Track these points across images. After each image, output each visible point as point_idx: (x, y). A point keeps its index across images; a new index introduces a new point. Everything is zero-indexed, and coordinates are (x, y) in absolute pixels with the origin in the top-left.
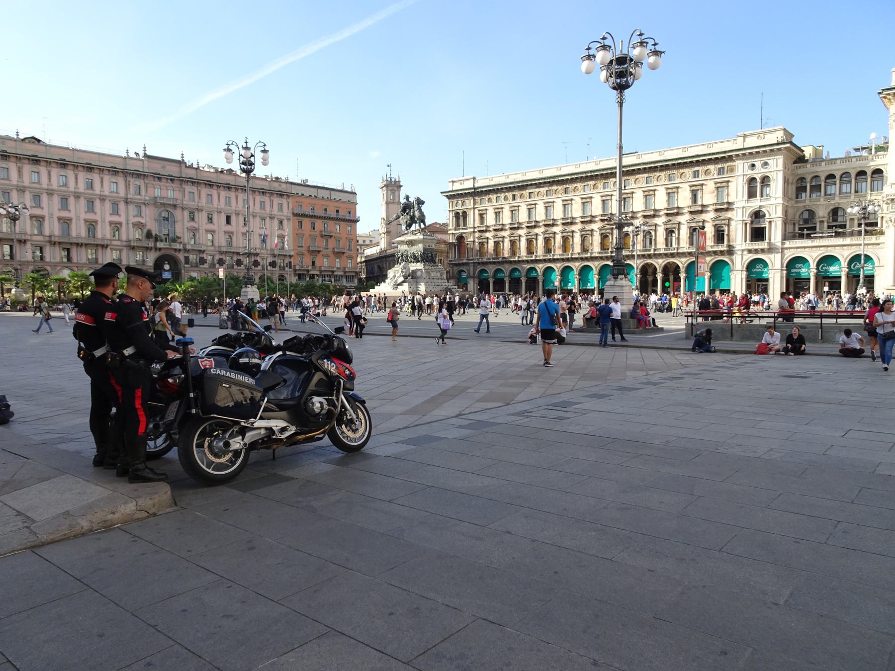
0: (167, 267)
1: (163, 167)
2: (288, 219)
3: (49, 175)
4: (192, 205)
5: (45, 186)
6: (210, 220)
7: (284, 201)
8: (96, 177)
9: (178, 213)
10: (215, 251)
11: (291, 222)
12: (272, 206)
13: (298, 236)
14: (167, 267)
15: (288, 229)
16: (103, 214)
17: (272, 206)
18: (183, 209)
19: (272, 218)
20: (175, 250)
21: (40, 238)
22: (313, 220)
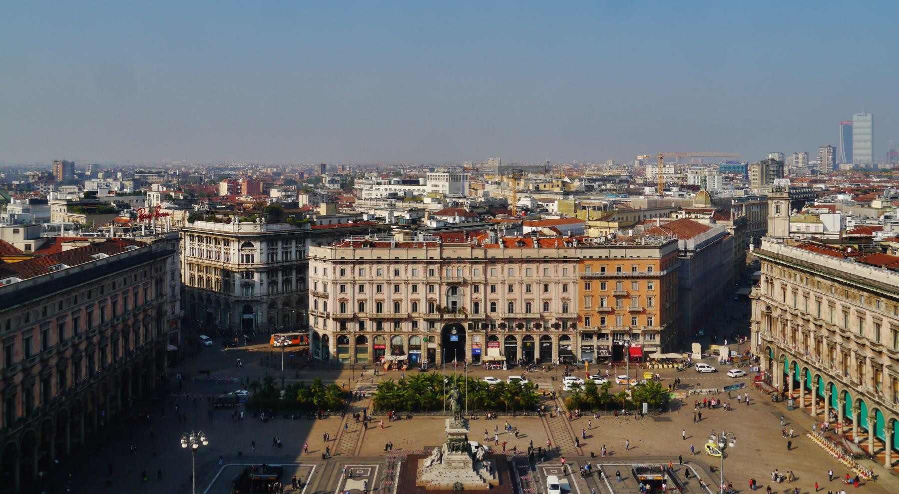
0: (454, 332)
2: (575, 283)
4: (475, 280)
5: (368, 278)
7: (570, 266)
8: (401, 267)
14: (454, 332)
15: (573, 292)
22: (604, 281)
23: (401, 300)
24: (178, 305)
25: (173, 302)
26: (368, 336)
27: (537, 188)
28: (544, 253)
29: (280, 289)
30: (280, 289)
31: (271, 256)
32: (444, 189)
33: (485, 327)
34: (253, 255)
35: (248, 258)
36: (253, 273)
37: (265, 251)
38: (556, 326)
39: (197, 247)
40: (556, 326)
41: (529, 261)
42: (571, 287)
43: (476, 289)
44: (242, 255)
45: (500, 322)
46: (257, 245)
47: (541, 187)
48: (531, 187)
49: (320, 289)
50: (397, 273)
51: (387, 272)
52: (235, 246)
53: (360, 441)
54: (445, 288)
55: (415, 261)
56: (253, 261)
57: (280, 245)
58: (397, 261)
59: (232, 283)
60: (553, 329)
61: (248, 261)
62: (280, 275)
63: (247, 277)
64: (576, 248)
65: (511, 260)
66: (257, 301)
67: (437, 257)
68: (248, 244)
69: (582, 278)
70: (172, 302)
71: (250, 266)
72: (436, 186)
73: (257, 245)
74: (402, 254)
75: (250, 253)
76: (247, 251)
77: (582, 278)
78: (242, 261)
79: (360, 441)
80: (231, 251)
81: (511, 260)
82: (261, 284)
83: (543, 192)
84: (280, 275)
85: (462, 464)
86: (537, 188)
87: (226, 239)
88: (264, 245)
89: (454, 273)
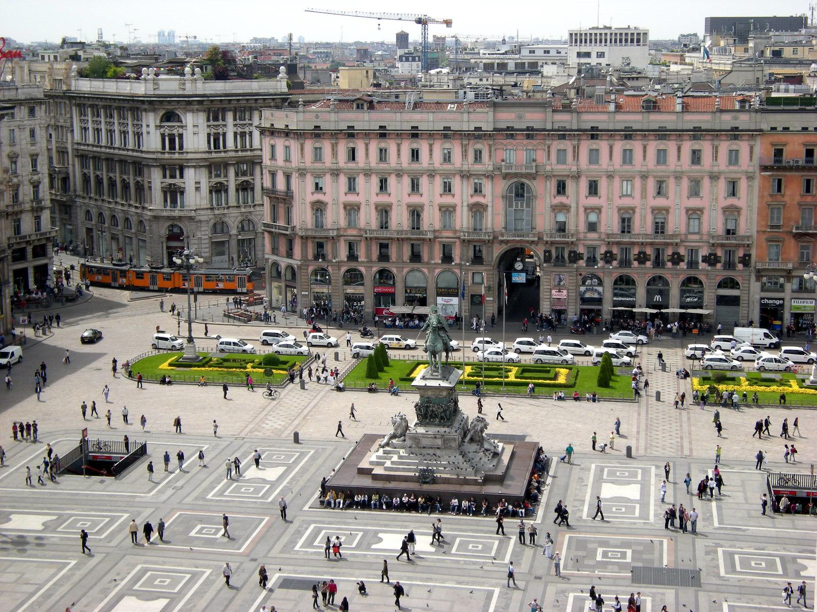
0: (519, 266)
1: (520, 117)
2: (750, 178)
3: (367, 150)
4: (561, 169)
6: (593, 189)
7: (743, 147)
8: (423, 146)
9: (537, 186)
10: (600, 239)
11: (756, 183)
12: (715, 157)
13: (772, 208)
16: (431, 195)
17: (715, 157)
18: (548, 177)
19: (714, 177)
20: (527, 242)
21: (354, 232)
23: (422, 206)
24: (46, 216)
25: (37, 210)
26: (363, 269)
27: (777, 54)
28: (692, 120)
29: (232, 201)
30: (232, 201)
31: (216, 140)
32: (600, 60)
33: (575, 257)
34: (181, 136)
35: (173, 142)
36: (181, 169)
37: (203, 131)
38: (711, 260)
39: (90, 125)
40: (711, 260)
41: (662, 133)
42: (743, 185)
43: (561, 188)
44: (163, 136)
45: (603, 250)
46: (189, 119)
47: (787, 53)
48: (768, 54)
49: (281, 186)
50: (415, 155)
51: (399, 154)
52: (150, 121)
53: (300, 418)
54: (502, 186)
55: (447, 134)
56: (181, 147)
57: (230, 116)
58: (415, 134)
59: (146, 185)
60: (702, 266)
61: (172, 147)
62: (232, 172)
63: (173, 176)
64: (756, 111)
65: (628, 134)
66: (191, 218)
67: (487, 126)
68: (169, 116)
69: (764, 168)
70: (33, 210)
71: (177, 156)
72: (588, 55)
73: (189, 119)
74: (426, 121)
75: (175, 132)
76: (171, 128)
77: (764, 168)
78: (164, 147)
79: (300, 418)
80: (144, 130)
81: (628, 134)
82: (198, 189)
83: (787, 63)
84: (232, 172)
85: (439, 442)
86: (777, 54)
87: (134, 107)
88: (201, 118)
89: (516, 155)
